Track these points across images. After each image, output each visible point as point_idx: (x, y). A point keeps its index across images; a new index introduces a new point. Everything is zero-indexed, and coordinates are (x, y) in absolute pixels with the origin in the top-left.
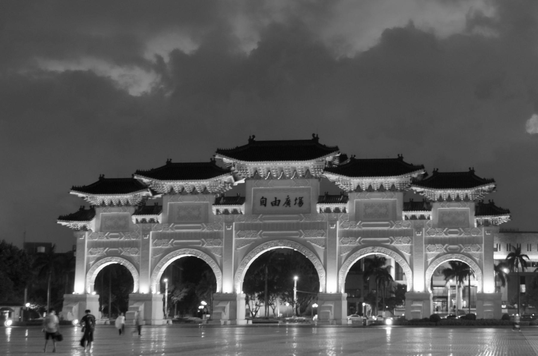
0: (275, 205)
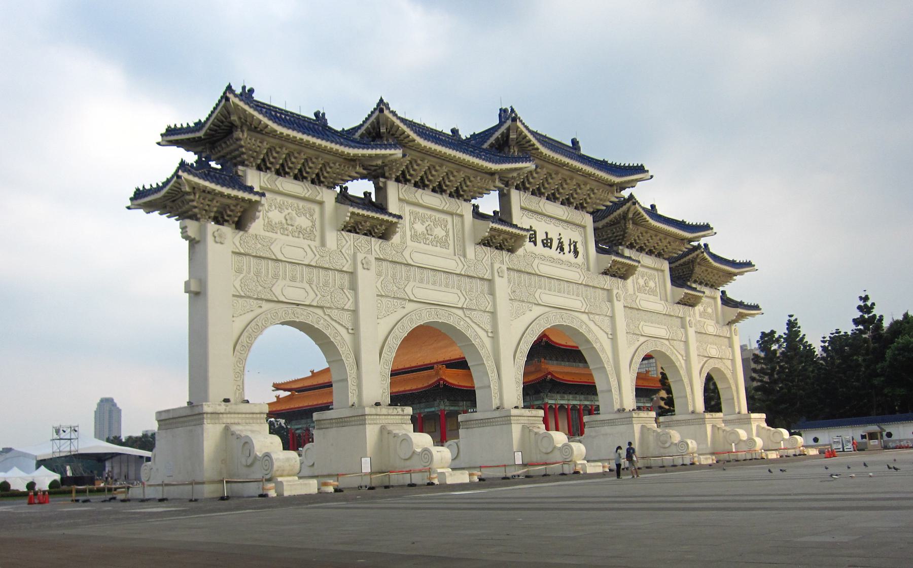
0: (547, 246)
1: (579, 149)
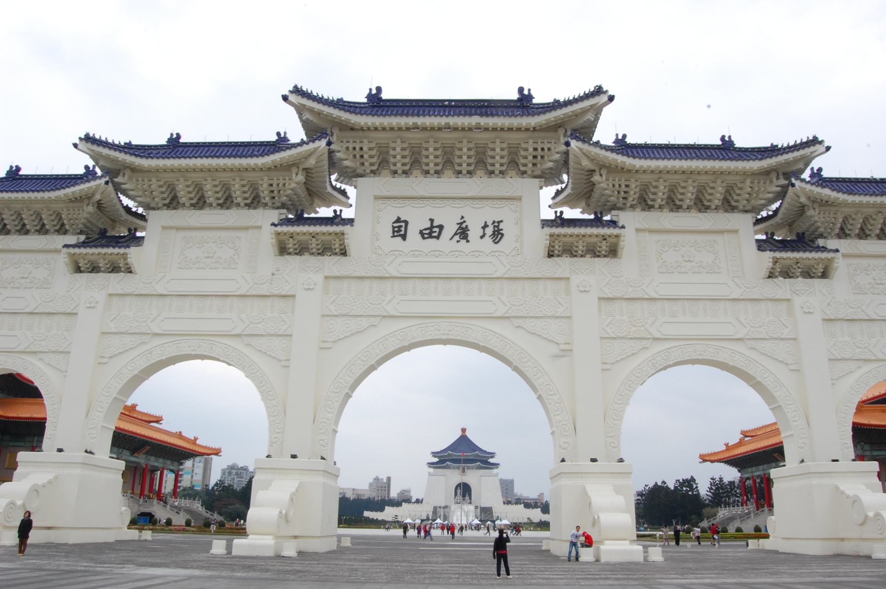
0: (430, 237)
1: (530, 97)
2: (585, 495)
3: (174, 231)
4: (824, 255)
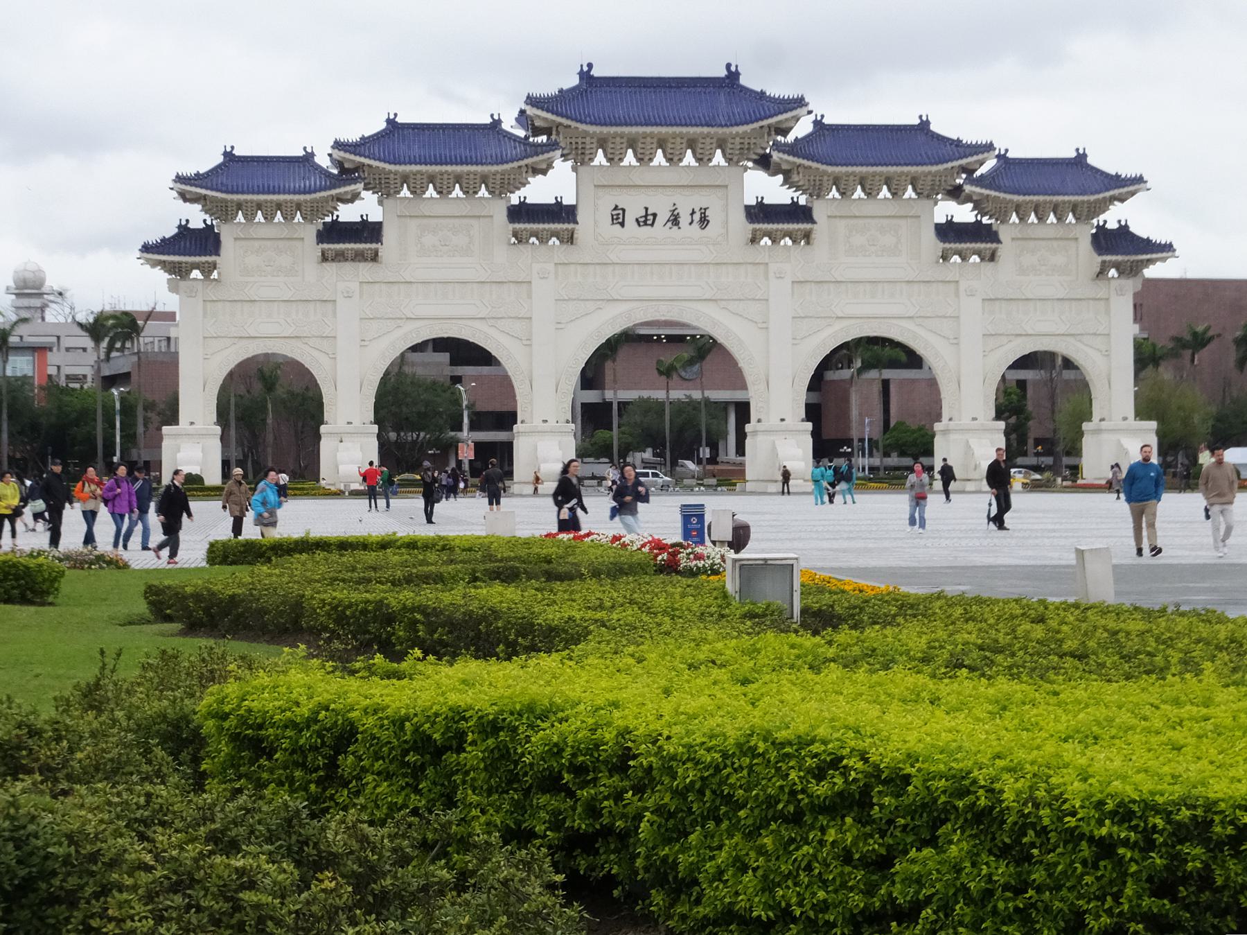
0: (646, 224)
2: (774, 448)
3: (408, 220)
4: (989, 245)
